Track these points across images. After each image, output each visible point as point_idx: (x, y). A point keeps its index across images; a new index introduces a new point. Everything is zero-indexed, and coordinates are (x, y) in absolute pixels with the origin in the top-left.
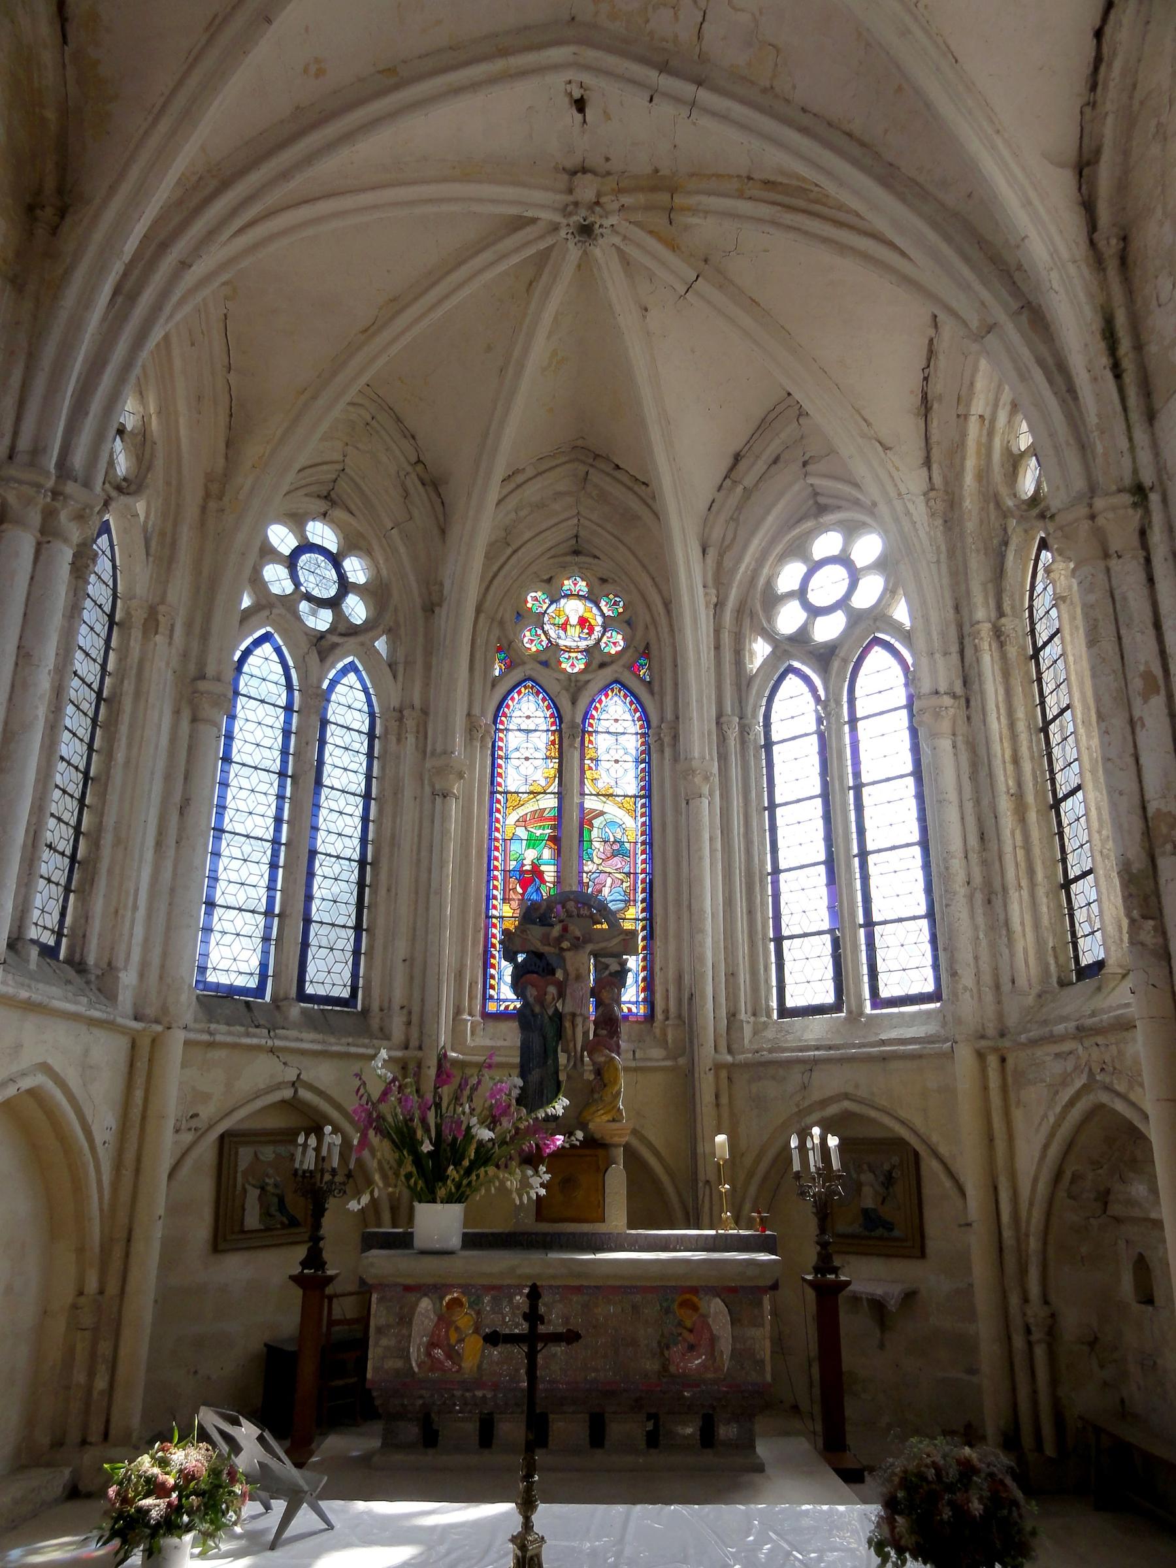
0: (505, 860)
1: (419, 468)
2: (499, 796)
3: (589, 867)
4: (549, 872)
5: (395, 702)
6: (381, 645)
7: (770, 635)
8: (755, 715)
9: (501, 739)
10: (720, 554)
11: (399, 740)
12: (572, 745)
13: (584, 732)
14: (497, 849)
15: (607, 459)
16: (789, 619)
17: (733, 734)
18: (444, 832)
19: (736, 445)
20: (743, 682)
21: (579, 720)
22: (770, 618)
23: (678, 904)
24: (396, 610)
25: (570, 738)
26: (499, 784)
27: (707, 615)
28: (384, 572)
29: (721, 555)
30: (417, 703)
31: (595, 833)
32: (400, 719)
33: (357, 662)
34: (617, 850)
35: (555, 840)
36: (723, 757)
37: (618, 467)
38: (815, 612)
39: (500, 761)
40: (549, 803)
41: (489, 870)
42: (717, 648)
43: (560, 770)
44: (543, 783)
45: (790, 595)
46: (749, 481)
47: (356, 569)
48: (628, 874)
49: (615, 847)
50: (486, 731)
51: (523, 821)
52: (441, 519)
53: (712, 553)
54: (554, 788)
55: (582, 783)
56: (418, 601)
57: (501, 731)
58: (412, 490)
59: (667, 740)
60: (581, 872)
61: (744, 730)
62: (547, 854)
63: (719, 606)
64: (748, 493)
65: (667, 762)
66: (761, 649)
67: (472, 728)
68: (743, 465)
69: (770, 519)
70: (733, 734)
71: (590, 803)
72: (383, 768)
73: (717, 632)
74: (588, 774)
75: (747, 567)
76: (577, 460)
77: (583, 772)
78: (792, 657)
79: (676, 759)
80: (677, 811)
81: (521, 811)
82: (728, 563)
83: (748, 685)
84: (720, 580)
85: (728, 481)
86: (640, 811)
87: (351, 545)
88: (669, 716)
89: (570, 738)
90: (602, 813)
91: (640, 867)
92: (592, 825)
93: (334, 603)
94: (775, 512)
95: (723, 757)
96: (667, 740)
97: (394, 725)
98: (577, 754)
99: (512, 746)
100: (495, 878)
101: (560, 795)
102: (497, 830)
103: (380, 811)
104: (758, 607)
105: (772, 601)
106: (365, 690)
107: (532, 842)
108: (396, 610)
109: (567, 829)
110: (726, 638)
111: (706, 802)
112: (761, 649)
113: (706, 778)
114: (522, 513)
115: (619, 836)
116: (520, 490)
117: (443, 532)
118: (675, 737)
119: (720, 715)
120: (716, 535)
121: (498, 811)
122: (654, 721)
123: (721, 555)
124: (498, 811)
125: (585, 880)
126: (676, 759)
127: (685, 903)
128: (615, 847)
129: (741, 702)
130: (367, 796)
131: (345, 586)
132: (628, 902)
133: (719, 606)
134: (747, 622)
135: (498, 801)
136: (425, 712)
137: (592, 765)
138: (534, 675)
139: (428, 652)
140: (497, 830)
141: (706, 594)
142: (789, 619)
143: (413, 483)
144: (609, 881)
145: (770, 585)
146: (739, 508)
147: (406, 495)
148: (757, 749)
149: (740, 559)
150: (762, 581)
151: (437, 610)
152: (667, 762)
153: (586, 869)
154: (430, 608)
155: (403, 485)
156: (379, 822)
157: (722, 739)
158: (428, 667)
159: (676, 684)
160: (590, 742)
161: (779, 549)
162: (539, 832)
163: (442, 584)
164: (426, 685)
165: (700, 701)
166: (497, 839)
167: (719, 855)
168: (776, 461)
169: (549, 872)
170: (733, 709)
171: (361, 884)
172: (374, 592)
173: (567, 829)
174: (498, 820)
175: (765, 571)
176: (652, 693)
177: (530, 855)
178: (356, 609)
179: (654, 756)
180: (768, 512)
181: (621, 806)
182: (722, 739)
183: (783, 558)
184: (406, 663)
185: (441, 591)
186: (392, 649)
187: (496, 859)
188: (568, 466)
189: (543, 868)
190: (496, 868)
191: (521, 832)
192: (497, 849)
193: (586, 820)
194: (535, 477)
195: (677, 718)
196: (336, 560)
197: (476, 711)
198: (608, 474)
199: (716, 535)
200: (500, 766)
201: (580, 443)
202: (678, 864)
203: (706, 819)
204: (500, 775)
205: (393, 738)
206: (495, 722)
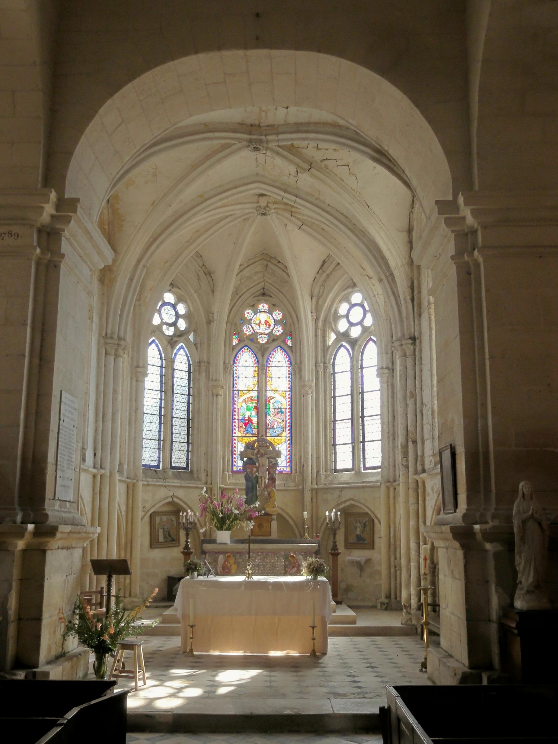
0: (238, 416)
1: (204, 268)
2: (235, 392)
3: (269, 418)
5: (197, 360)
6: (191, 337)
8: (329, 363)
9: (236, 370)
10: (317, 298)
11: (199, 374)
12: (262, 373)
13: (267, 366)
14: (235, 411)
18: (217, 409)
19: (323, 258)
20: (325, 349)
21: (265, 363)
23: (300, 432)
25: (262, 369)
26: (236, 387)
27: (312, 324)
28: (192, 309)
29: (318, 299)
31: (271, 405)
32: (200, 366)
33: (183, 345)
34: (279, 411)
37: (279, 262)
39: (236, 378)
40: (254, 394)
41: (233, 419)
42: (316, 336)
43: (258, 382)
44: (252, 386)
46: (328, 272)
48: (283, 420)
49: (279, 410)
50: (230, 368)
51: (245, 401)
52: (212, 287)
54: (256, 388)
55: (266, 386)
56: (204, 320)
57: (236, 367)
60: (266, 420)
62: (254, 413)
63: (317, 320)
64: (328, 276)
67: (225, 368)
68: (326, 265)
69: (336, 287)
71: (269, 394)
72: (194, 384)
73: (316, 329)
74: (268, 383)
75: (328, 305)
76: (263, 259)
77: (266, 382)
80: (300, 398)
84: (317, 309)
86: (288, 396)
88: (298, 362)
89: (262, 369)
90: (274, 398)
91: (288, 418)
92: (270, 402)
94: (338, 285)
96: (297, 371)
97: (197, 368)
98: (264, 376)
99: (240, 373)
100: (235, 422)
101: (259, 392)
102: (235, 404)
103: (194, 400)
105: (337, 317)
107: (248, 409)
108: (196, 323)
109: (261, 404)
110: (319, 332)
114: (242, 281)
115: (280, 406)
116: (241, 273)
117: (213, 291)
118: (300, 370)
120: (316, 292)
121: (236, 397)
122: (293, 363)
123: (318, 299)
124: (236, 397)
125: (268, 423)
127: (302, 433)
128: (279, 410)
129: (324, 356)
130: (189, 395)
132: (284, 428)
133: (317, 320)
134: (327, 325)
135: (236, 394)
136: (209, 363)
137: (270, 379)
138: (249, 345)
140: (235, 404)
141: (312, 316)
143: (201, 274)
144: (276, 423)
145: (336, 312)
146: (325, 281)
148: (330, 374)
151: (212, 323)
153: (268, 419)
154: (209, 322)
156: (193, 404)
158: (209, 346)
160: (269, 370)
161: (339, 298)
162: (250, 405)
163: (213, 314)
164: (209, 352)
166: (235, 408)
167: (315, 415)
169: (255, 420)
170: (321, 360)
171: (188, 427)
172: (187, 317)
173: (261, 404)
174: (235, 401)
175: (335, 306)
176: (292, 351)
177: (247, 414)
178: (182, 325)
179: (293, 376)
180: (335, 284)
181: (281, 395)
183: (341, 301)
185: (213, 317)
187: (235, 415)
188: (260, 262)
189: (252, 418)
190: (235, 419)
191: (244, 405)
192: (235, 411)
193: (267, 401)
194: (247, 267)
198: (275, 265)
199: (316, 292)
200: (236, 380)
204: (236, 384)
205: (197, 373)
206: (233, 364)
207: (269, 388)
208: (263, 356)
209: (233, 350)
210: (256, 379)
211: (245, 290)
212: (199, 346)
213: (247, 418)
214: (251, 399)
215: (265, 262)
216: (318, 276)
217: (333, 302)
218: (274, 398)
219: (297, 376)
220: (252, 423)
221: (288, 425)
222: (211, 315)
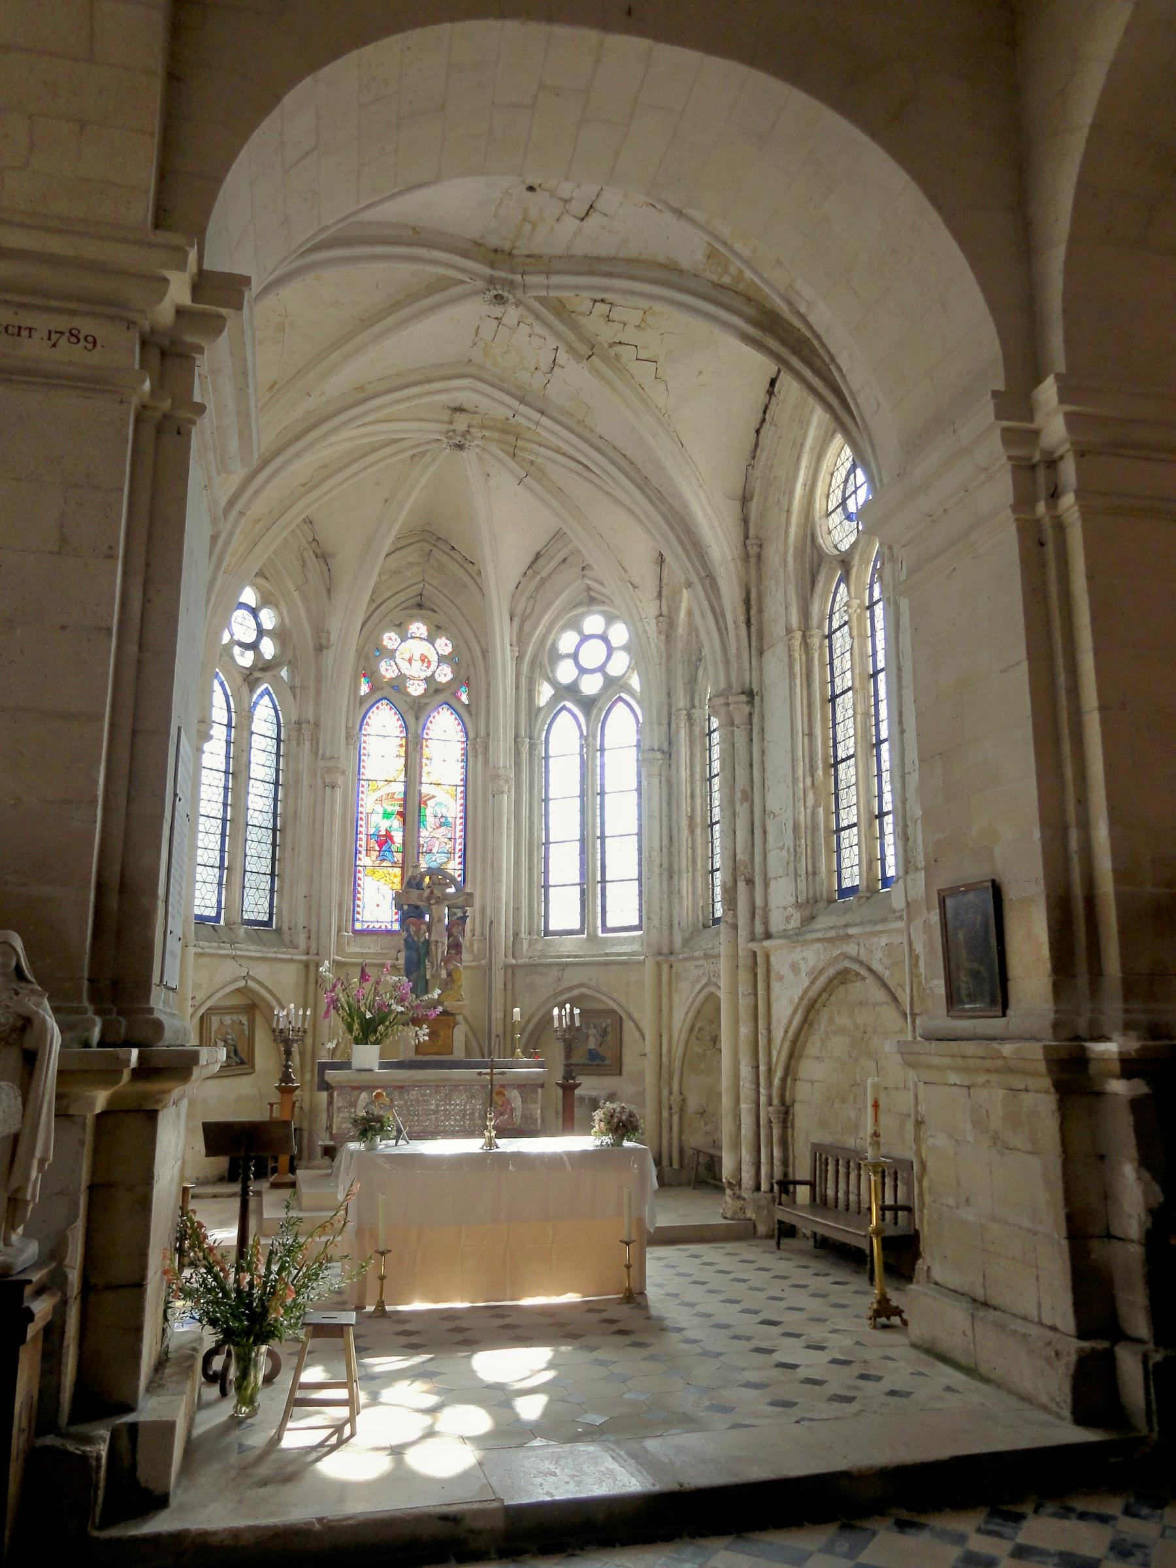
3: (424, 833)
4: (398, 837)
5: (294, 718)
6: (284, 673)
7: (554, 683)
10: (523, 621)
11: (298, 744)
12: (415, 750)
15: (446, 541)
16: (565, 672)
17: (525, 750)
20: (534, 712)
22: (553, 671)
24: (294, 648)
28: (287, 621)
29: (523, 622)
30: (311, 720)
32: (300, 729)
34: (443, 822)
35: (401, 814)
36: (518, 765)
38: (583, 671)
40: (399, 788)
42: (517, 688)
43: (406, 766)
45: (568, 656)
47: (268, 618)
48: (450, 839)
53: (517, 620)
54: (402, 778)
58: (308, 561)
59: (480, 750)
61: (532, 747)
62: (396, 823)
63: (519, 659)
64: (543, 581)
65: (479, 765)
66: (545, 693)
68: (541, 561)
70: (525, 750)
74: (425, 769)
76: (424, 540)
77: (421, 767)
78: (565, 699)
79: (486, 762)
80: (485, 800)
81: (379, 794)
82: (527, 628)
83: (537, 715)
84: (521, 639)
85: (530, 572)
87: (266, 600)
88: (482, 733)
90: (434, 797)
93: (254, 646)
94: (561, 598)
95: (518, 765)
96: (480, 750)
97: (294, 734)
100: (361, 839)
101: (407, 784)
103: (286, 794)
104: (546, 661)
106: (275, 708)
107: (387, 815)
108: (294, 648)
109: (410, 809)
110: (524, 682)
111: (505, 796)
112: (545, 693)
113: (507, 781)
114: (384, 578)
118: (486, 749)
119: (516, 737)
120: (519, 609)
122: (471, 736)
126: (486, 762)
128: (443, 820)
129: (531, 726)
131: (261, 632)
134: (537, 671)
136: (317, 725)
138: (389, 696)
139: (319, 680)
141: (512, 651)
142: (565, 672)
144: (437, 843)
145: (554, 647)
146: (537, 589)
147: (304, 564)
149: (535, 628)
150: (550, 642)
151: (325, 651)
152: (479, 765)
154: (320, 648)
155: (302, 556)
156: (284, 801)
157: (518, 753)
158: (318, 692)
159: (488, 711)
161: (562, 622)
162: (390, 809)
163: (329, 633)
165: (505, 728)
168: (564, 560)
169: (398, 837)
172: (280, 635)
173: (410, 809)
177: (384, 825)
178: (268, 648)
179: (470, 759)
182: (518, 753)
183: (563, 629)
184: (301, 687)
186: (292, 673)
188: (419, 545)
193: (422, 802)
195: (488, 735)
196: (254, 612)
197: (350, 725)
199: (519, 609)
201: (427, 528)
202: (485, 834)
203: (505, 808)
205: (294, 743)
207: (424, 780)
208: (417, 718)
209: (361, 704)
210: (403, 761)
211: (389, 594)
212: (298, 691)
213: (383, 833)
214: (391, 796)
215: (427, 547)
216: (524, 580)
217: (549, 629)
218: (434, 797)
219: (480, 758)
220: (393, 842)
221: (458, 847)
222: (324, 635)
